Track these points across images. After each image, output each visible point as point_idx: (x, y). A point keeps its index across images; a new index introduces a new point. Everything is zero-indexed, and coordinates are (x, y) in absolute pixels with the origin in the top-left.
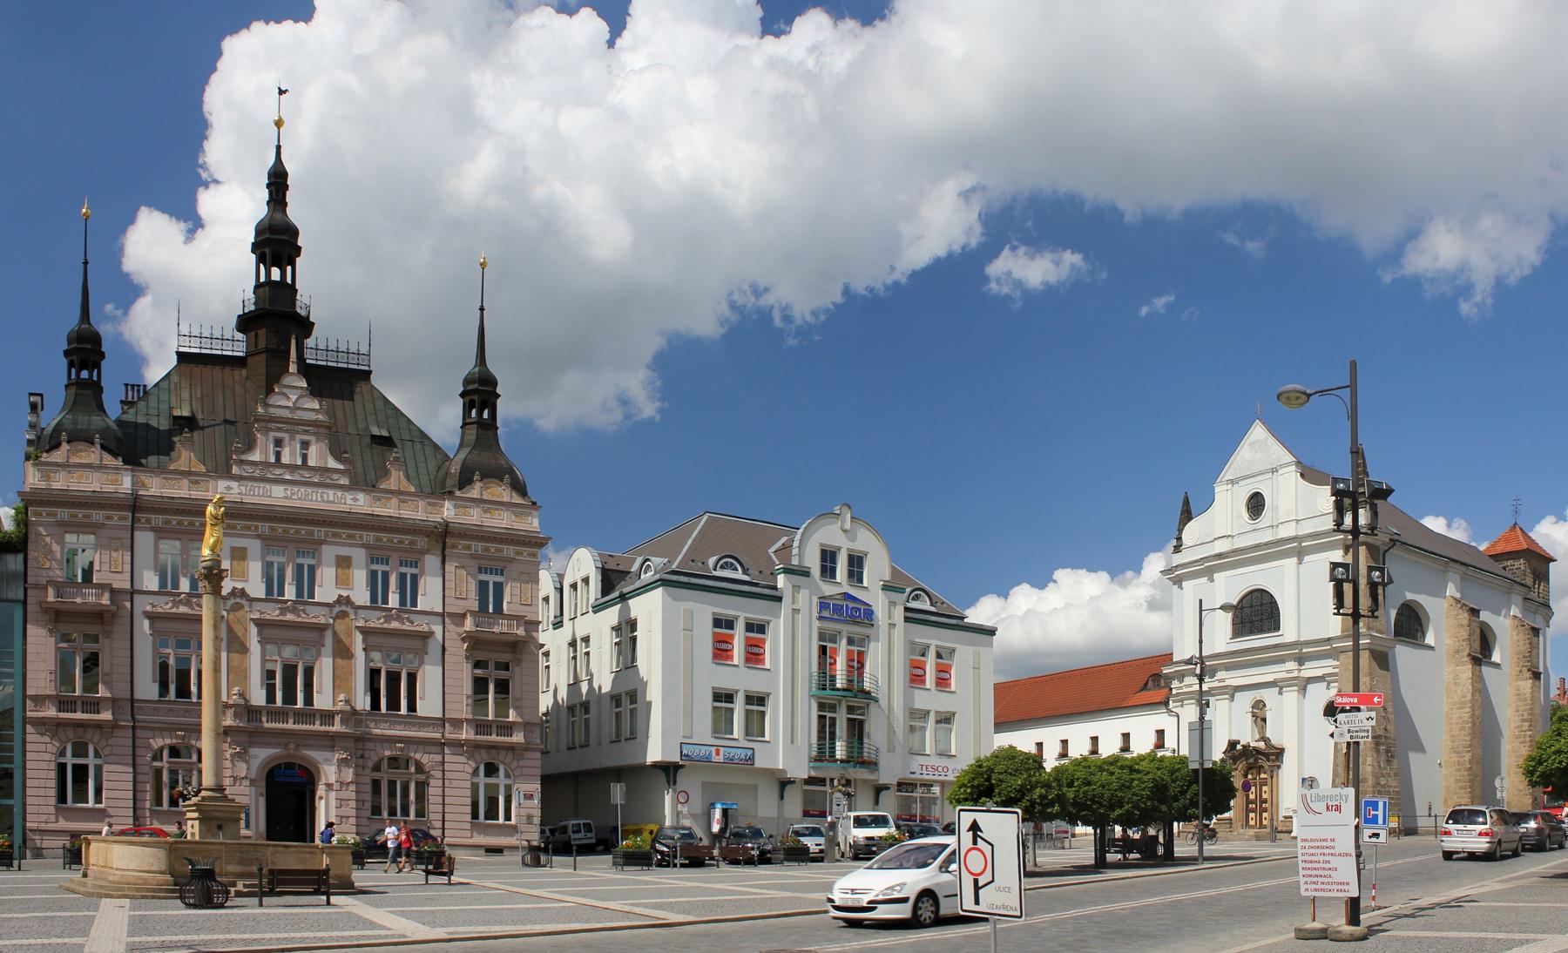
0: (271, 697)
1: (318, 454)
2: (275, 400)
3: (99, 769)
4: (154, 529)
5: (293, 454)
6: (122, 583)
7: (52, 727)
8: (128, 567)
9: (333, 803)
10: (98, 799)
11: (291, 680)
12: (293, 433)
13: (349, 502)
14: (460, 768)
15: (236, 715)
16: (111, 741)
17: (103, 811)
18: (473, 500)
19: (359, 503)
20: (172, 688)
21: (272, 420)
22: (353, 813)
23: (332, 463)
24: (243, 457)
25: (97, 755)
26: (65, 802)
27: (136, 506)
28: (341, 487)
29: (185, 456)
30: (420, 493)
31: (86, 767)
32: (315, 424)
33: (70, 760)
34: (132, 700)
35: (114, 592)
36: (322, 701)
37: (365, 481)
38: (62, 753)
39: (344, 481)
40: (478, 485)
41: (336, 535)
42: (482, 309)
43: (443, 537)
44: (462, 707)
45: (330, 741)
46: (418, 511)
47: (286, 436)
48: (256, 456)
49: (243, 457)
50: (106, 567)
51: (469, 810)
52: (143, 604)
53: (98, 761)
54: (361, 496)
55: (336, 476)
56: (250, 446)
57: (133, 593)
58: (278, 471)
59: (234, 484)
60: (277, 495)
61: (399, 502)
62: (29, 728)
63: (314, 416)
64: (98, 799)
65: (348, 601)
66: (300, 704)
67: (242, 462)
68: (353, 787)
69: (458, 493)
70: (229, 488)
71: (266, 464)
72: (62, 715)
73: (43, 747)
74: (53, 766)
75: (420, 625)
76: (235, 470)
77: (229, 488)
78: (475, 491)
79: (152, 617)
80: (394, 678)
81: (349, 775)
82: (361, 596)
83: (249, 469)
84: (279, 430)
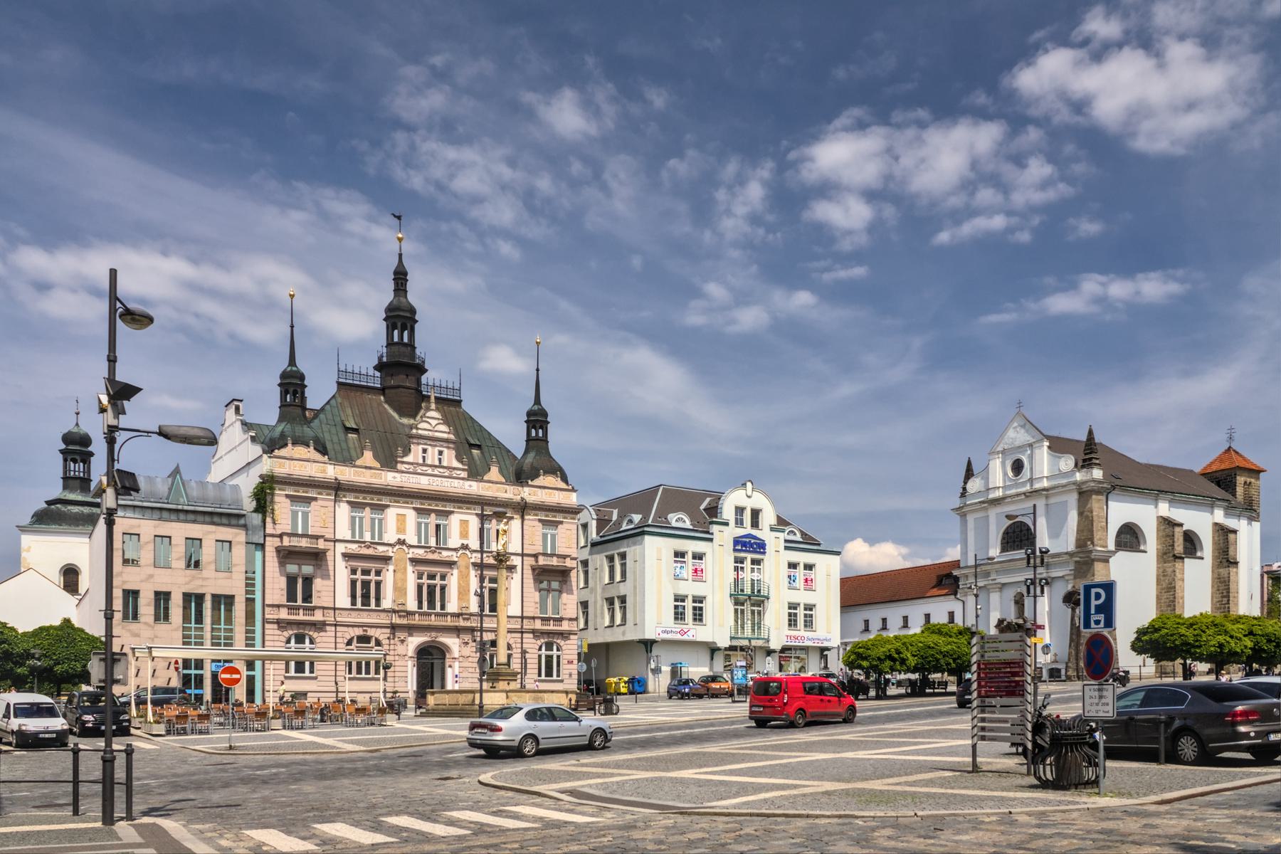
0: (420, 606)
1: (449, 457)
4: (348, 502)
11: (431, 595)
17: (315, 678)
19: (473, 488)
20: (359, 600)
23: (456, 464)
24: (405, 459)
25: (312, 642)
27: (338, 488)
30: (508, 482)
32: (447, 441)
36: (452, 607)
37: (475, 473)
39: (464, 474)
43: (523, 508)
45: (457, 631)
46: (511, 493)
48: (409, 458)
54: (474, 484)
56: (407, 451)
60: (423, 483)
61: (495, 486)
62: (267, 626)
63: (445, 436)
64: (312, 672)
66: (438, 609)
78: (541, 481)
79: (348, 556)
82: (474, 543)
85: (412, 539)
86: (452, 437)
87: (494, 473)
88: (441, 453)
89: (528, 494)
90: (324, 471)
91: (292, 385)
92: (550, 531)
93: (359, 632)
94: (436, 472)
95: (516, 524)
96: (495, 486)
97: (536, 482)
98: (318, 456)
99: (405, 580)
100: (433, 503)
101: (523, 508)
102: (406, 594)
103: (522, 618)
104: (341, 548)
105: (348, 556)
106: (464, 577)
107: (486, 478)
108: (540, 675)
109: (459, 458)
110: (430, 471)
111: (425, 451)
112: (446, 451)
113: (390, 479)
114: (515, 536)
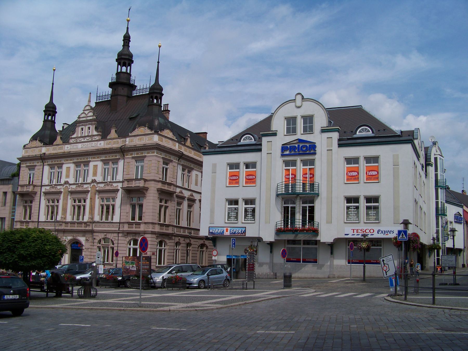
4: (49, 165)
8: (41, 178)
12: (85, 125)
18: (135, 136)
19: (102, 145)
23: (95, 133)
24: (73, 137)
28: (97, 141)
32: (91, 120)
37: (104, 137)
41: (94, 158)
42: (158, 62)
48: (74, 136)
49: (73, 137)
54: (102, 142)
55: (96, 137)
59: (69, 146)
60: (79, 147)
63: (91, 118)
67: (72, 138)
69: (130, 134)
70: (68, 148)
80: (108, 208)
83: (73, 140)
84: (82, 125)
87: (113, 133)
88: (89, 128)
90: (41, 151)
91: (50, 110)
92: (140, 164)
94: (86, 140)
97: (134, 133)
99: (67, 204)
100: (82, 158)
101: (123, 151)
102: (66, 211)
104: (44, 189)
105: (46, 193)
106: (66, 199)
107: (108, 137)
109: (96, 129)
112: (91, 126)
113: (67, 148)
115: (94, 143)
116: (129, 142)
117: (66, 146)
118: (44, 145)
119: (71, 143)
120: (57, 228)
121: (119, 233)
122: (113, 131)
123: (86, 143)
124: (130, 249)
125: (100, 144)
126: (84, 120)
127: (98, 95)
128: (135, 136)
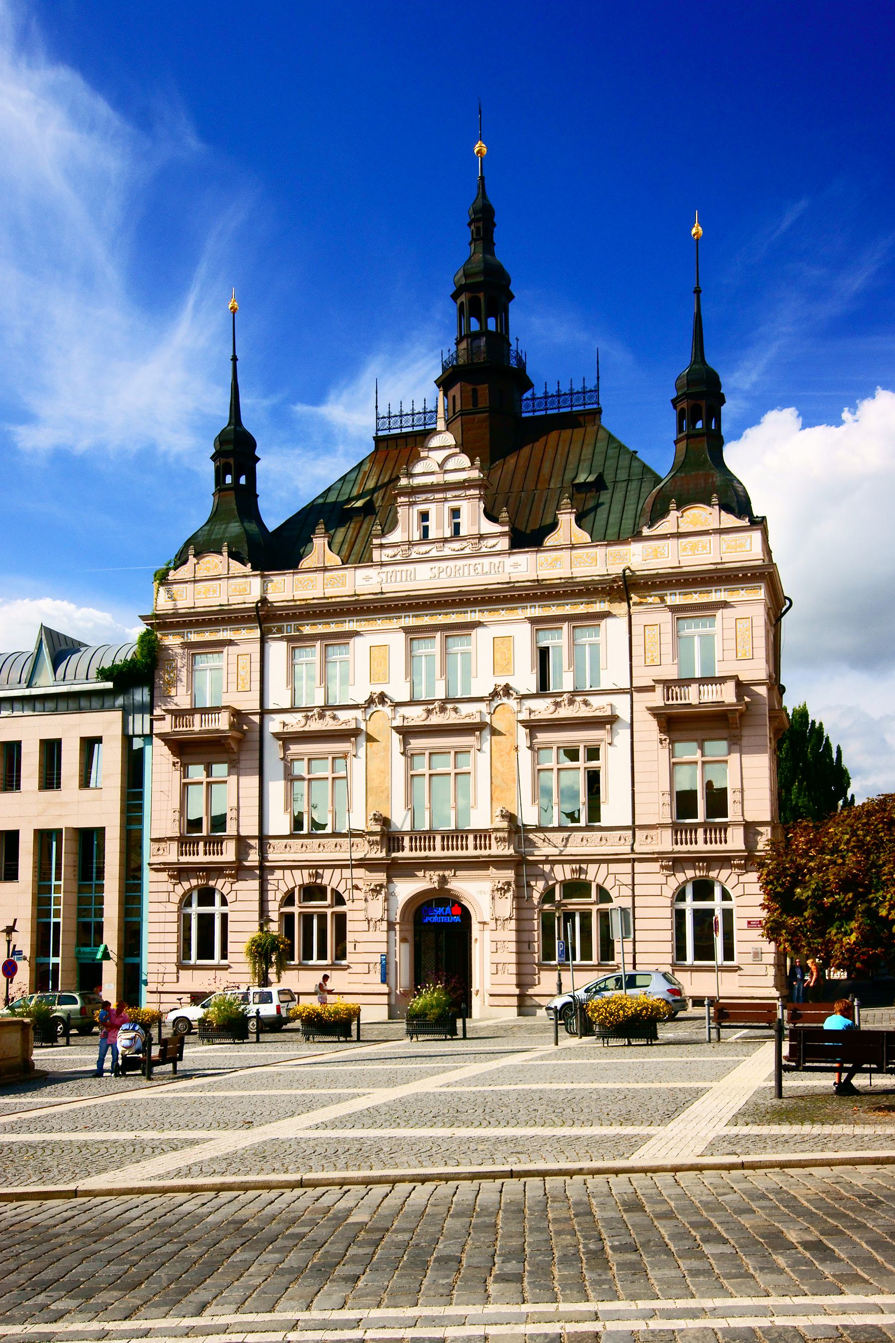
2: (419, 468)
3: (224, 917)
5: (440, 526)
6: (249, 703)
7: (180, 873)
8: (256, 686)
9: (488, 947)
10: (224, 956)
13: (508, 569)
14: (656, 890)
15: (371, 843)
16: (235, 886)
18: (664, 537)
21: (413, 491)
22: (513, 958)
24: (384, 541)
25: (224, 902)
26: (187, 955)
27: (265, 617)
29: (320, 550)
31: (212, 916)
33: (195, 910)
34: (263, 838)
35: (238, 715)
37: (527, 537)
38: (189, 904)
40: (674, 514)
43: (626, 587)
44: (657, 808)
47: (432, 508)
48: (396, 536)
50: (232, 687)
51: (668, 947)
52: (274, 725)
53: (225, 909)
56: (390, 525)
57: (263, 712)
58: (424, 548)
59: (372, 572)
64: (224, 956)
65: (507, 690)
67: (382, 546)
68: (512, 924)
70: (367, 578)
71: (411, 544)
72: (184, 859)
73: (164, 897)
74: (174, 917)
75: (599, 705)
76: (376, 555)
77: (367, 578)
78: (667, 525)
81: (506, 906)
83: (390, 552)
84: (426, 501)
85: (399, 691)
86: (475, 474)
89: (638, 557)
93: (302, 878)
95: (614, 630)
96: (572, 554)
98: (237, 567)
103: (633, 828)
108: (680, 953)
109: (492, 517)
110: (434, 553)
111: (424, 516)
114: (621, 654)
115: (486, 561)
116: (638, 557)
117: (362, 573)
118: (254, 568)
119: (382, 564)
120: (356, 856)
121: (634, 860)
122: (566, 519)
123: (451, 564)
124: (680, 915)
125: (516, 565)
126: (425, 486)
127: (383, 412)
128: (664, 537)
